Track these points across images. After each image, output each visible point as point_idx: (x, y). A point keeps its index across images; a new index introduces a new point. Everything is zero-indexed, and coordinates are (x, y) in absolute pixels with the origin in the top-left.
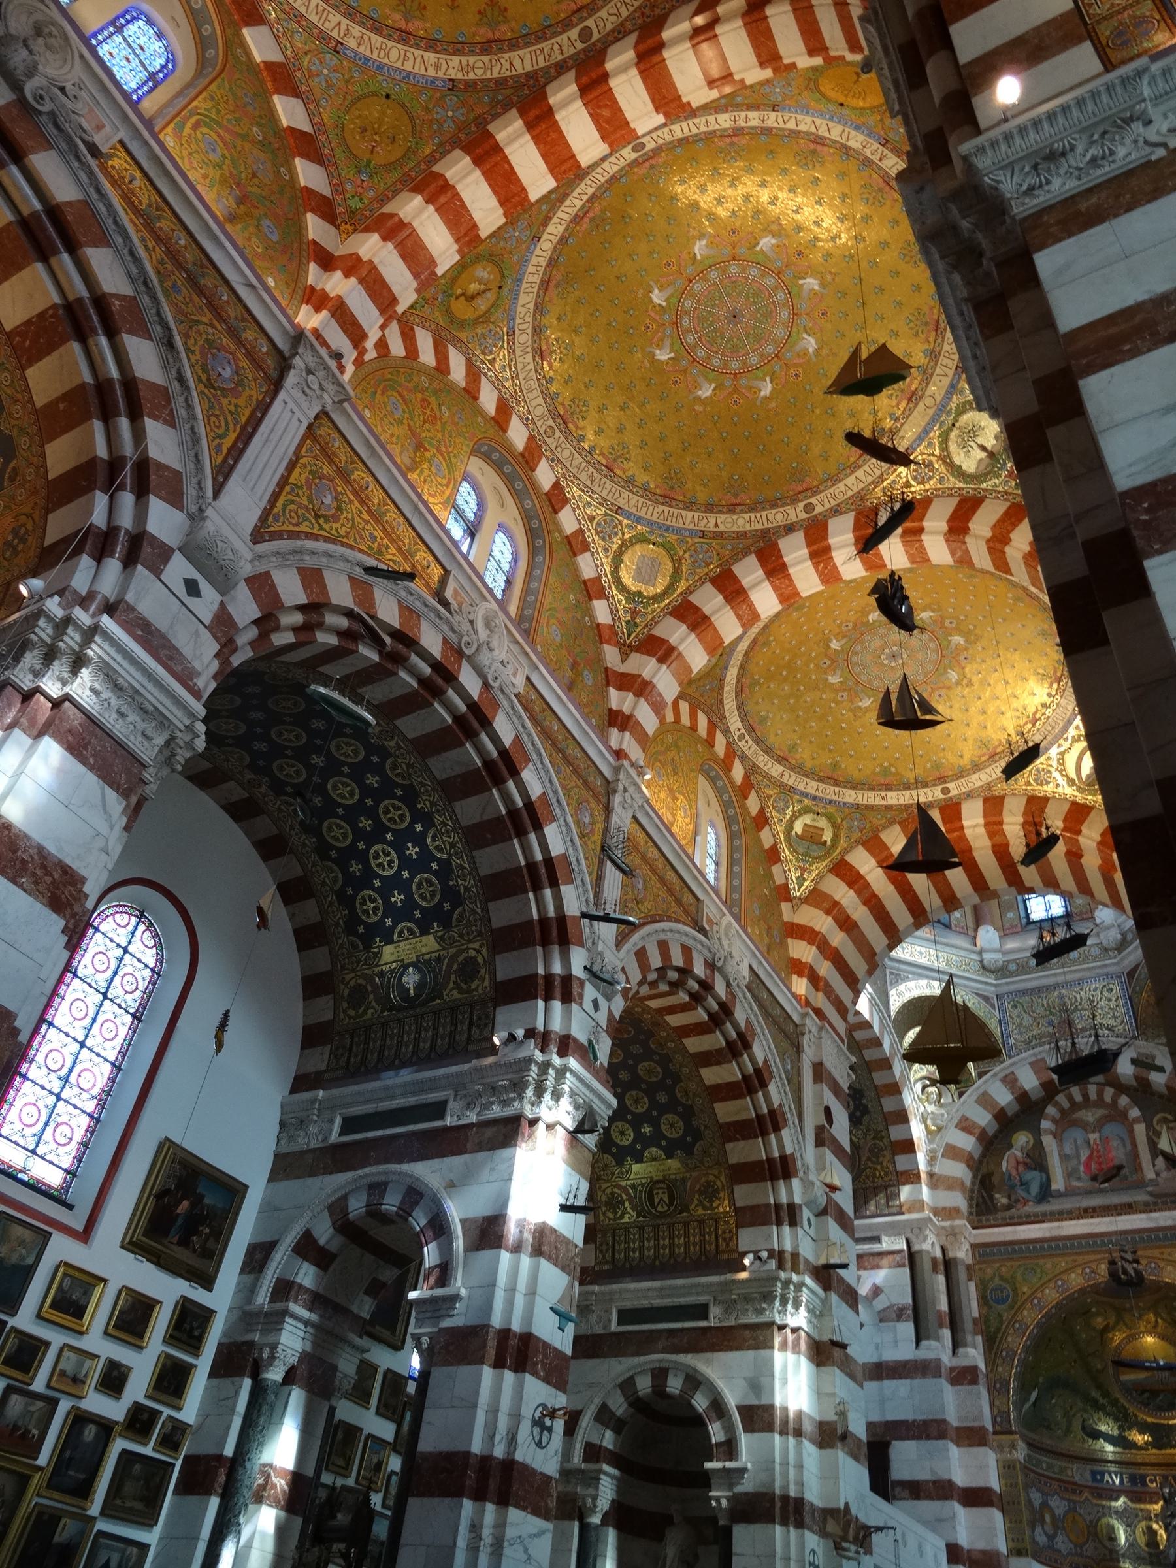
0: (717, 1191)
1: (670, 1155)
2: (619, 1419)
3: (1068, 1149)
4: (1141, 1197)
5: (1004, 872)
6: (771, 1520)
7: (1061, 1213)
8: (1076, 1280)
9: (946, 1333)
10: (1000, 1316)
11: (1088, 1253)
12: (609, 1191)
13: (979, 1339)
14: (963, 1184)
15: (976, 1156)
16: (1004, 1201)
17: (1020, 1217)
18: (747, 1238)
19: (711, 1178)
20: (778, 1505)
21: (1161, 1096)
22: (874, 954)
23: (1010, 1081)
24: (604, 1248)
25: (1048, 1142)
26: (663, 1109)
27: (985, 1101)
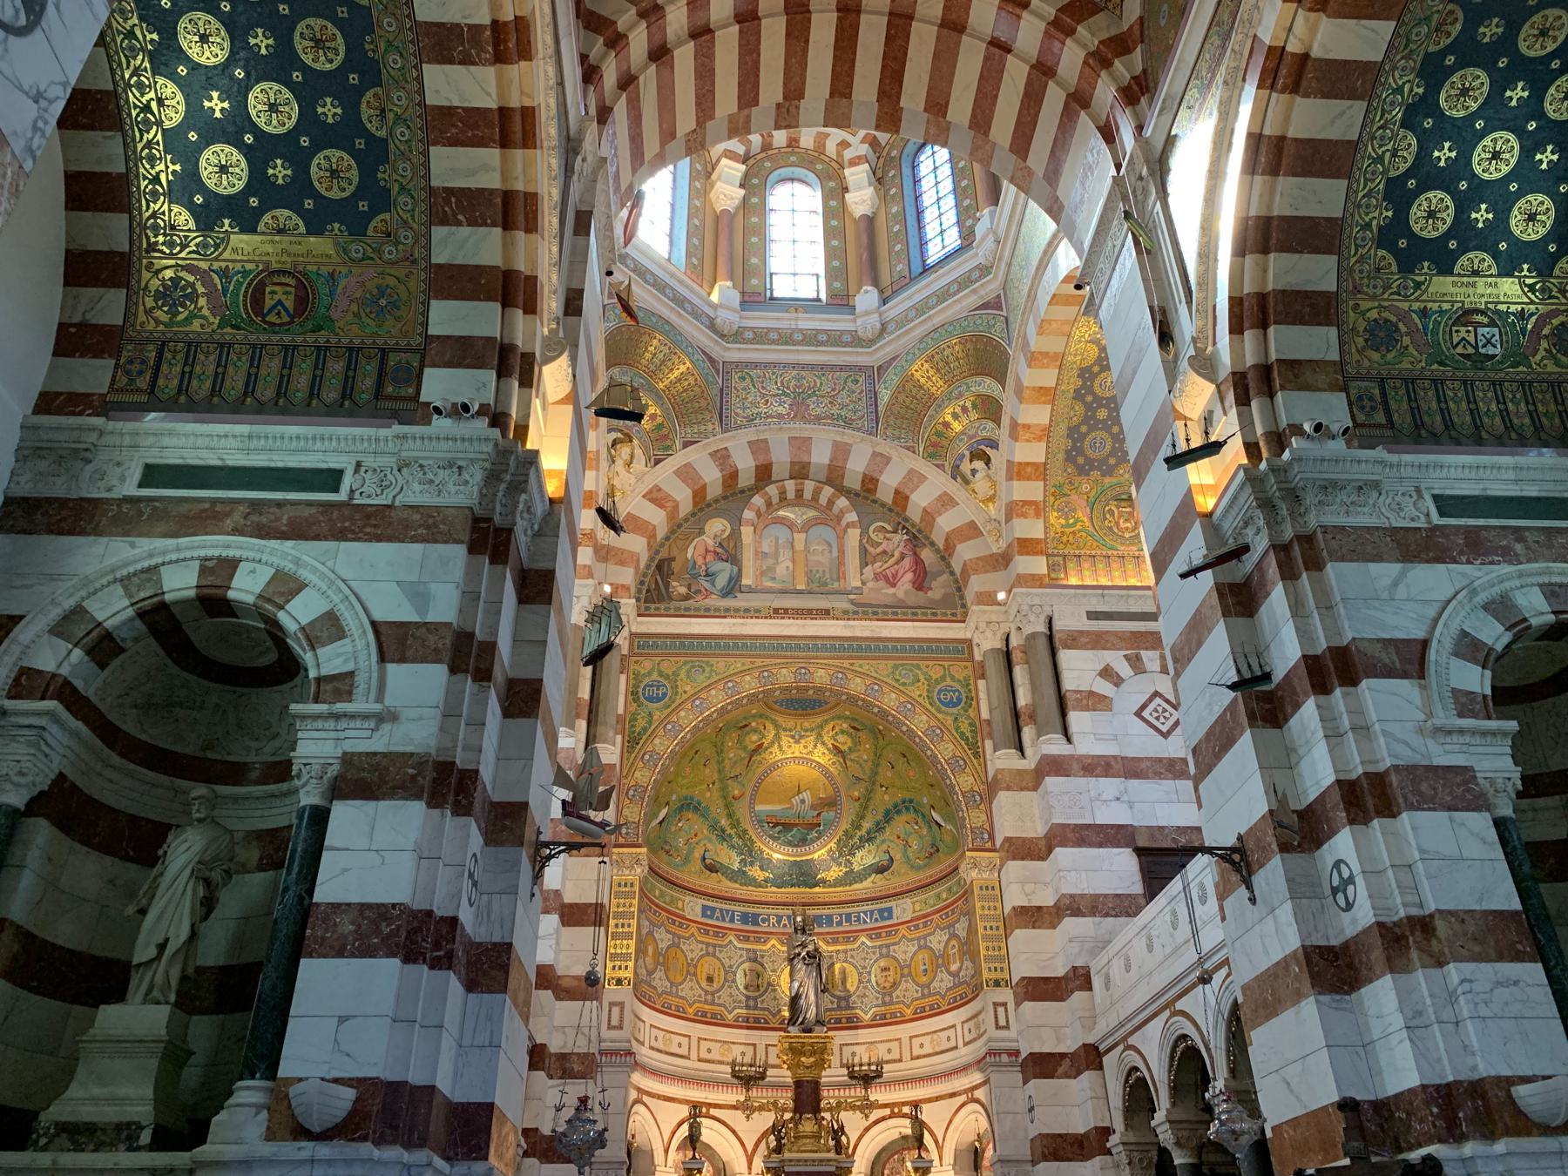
0: (394, 305)
1: (315, 228)
2: (108, 636)
3: (766, 547)
4: (840, 604)
5: (884, 67)
6: (417, 796)
7: (747, 610)
8: (750, 684)
9: (582, 725)
10: (650, 715)
11: (772, 657)
12: (169, 274)
13: (619, 738)
14: (638, 561)
15: (660, 534)
16: (683, 590)
17: (696, 609)
18: (438, 384)
19: (392, 282)
20: (430, 774)
21: (883, 505)
22: (673, 135)
23: (721, 457)
24: (136, 367)
25: (747, 532)
26: (325, 136)
27: (686, 473)
